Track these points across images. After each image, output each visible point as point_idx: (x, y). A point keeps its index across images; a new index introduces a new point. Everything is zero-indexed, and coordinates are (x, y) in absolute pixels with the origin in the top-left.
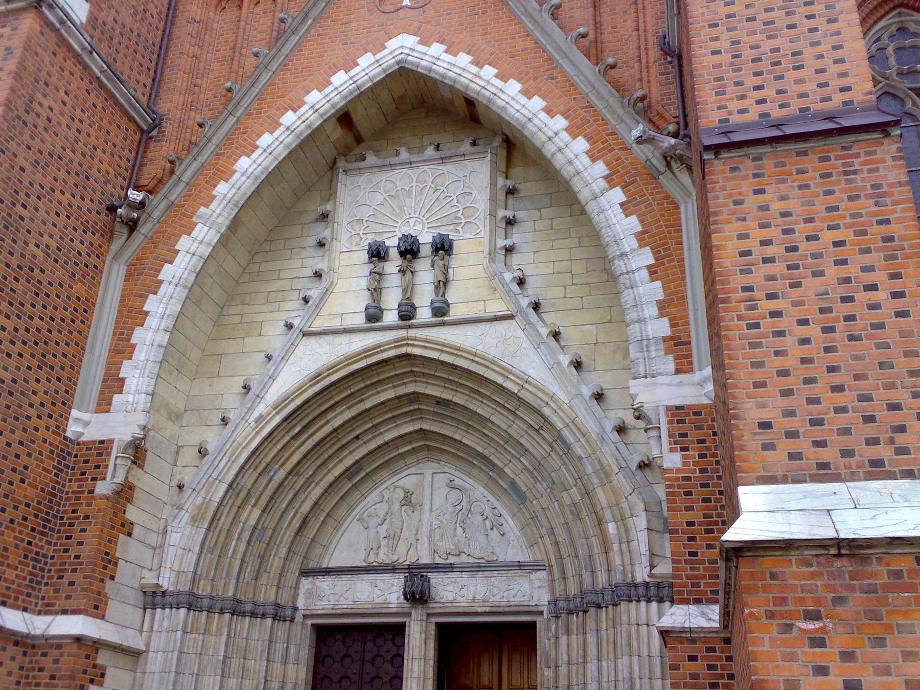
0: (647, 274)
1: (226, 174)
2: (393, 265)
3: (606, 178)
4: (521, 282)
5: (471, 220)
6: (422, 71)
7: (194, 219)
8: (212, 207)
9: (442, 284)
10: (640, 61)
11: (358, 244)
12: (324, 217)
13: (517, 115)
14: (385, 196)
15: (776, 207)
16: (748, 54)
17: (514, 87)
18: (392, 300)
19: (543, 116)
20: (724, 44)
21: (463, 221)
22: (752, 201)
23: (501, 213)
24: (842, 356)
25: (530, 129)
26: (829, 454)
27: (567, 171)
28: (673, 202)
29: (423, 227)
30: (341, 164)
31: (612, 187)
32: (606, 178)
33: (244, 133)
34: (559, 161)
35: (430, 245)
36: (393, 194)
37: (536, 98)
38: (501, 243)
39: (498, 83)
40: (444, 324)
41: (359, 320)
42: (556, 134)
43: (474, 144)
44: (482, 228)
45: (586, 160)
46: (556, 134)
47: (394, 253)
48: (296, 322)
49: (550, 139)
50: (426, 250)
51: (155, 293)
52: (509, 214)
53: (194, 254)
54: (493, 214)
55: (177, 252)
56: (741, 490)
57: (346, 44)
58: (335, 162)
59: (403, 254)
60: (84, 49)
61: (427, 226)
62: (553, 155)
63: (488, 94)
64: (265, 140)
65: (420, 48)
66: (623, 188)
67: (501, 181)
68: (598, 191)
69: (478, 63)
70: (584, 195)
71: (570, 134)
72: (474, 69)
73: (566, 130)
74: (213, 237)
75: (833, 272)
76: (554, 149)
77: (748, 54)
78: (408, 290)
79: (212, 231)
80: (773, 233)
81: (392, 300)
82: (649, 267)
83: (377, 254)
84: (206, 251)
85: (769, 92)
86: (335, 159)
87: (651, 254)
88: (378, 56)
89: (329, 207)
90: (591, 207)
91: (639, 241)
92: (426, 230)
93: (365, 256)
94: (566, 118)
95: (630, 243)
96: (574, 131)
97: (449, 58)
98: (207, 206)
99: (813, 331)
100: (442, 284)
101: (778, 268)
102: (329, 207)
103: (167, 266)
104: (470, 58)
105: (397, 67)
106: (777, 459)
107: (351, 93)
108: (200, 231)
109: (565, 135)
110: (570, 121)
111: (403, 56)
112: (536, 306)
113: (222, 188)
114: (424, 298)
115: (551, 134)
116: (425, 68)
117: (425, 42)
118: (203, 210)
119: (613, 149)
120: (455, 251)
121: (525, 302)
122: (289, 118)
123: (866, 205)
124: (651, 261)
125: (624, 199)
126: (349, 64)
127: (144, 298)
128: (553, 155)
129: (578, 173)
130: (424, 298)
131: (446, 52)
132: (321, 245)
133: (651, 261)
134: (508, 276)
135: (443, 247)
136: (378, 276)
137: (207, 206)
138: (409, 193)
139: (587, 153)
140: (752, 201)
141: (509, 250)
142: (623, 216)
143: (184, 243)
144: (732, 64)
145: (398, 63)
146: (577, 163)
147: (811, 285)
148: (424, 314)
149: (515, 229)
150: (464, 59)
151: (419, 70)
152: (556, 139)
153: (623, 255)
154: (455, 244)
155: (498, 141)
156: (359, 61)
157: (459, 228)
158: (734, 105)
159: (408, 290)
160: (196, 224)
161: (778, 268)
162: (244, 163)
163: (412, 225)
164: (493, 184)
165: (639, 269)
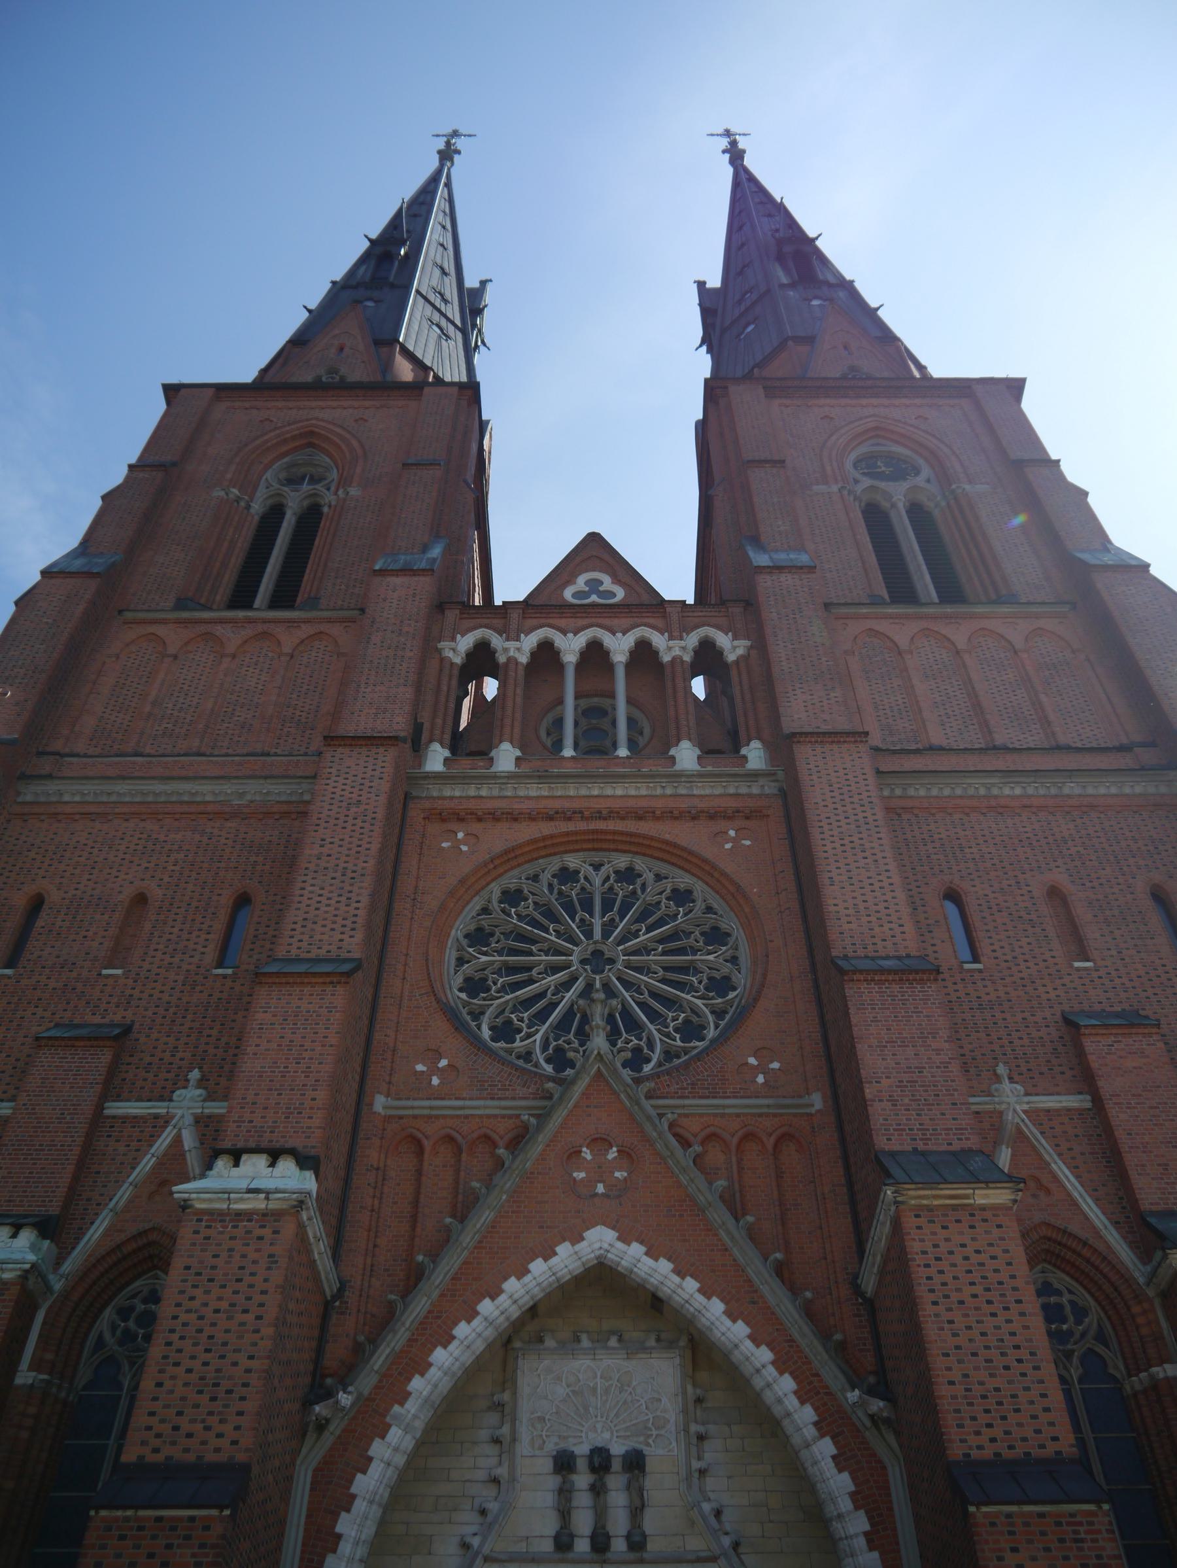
0: (865, 1542)
1: (423, 1367)
2: (582, 1480)
3: (816, 1424)
4: (718, 1513)
5: (662, 1432)
6: (623, 1271)
7: (388, 1419)
8: (408, 1405)
9: (637, 1511)
10: (831, 1294)
11: (541, 1448)
12: (499, 1406)
13: (723, 1338)
14: (567, 1390)
17: (717, 1307)
18: (583, 1523)
19: (749, 1344)
20: (956, 1375)
21: (654, 1433)
23: (694, 1428)
25: (736, 1356)
27: (777, 1411)
28: (880, 1461)
29: (612, 1433)
30: (517, 1344)
31: (822, 1436)
32: (816, 1424)
33: (438, 1317)
34: (768, 1397)
35: (621, 1459)
36: (577, 1389)
37: (740, 1323)
38: (696, 1465)
39: (701, 1298)
40: (641, 1561)
41: (548, 1546)
42: (764, 1366)
43: (658, 1340)
44: (674, 1444)
45: (795, 1402)
46: (764, 1366)
47: (582, 1464)
48: (476, 1542)
49: (758, 1371)
50: (616, 1465)
51: (348, 1510)
52: (701, 1429)
53: (389, 1464)
54: (686, 1430)
55: (370, 1459)
57: (542, 1227)
58: (509, 1341)
59: (593, 1469)
60: (315, 1237)
61: (615, 1434)
62: (762, 1390)
63: (692, 1309)
64: (462, 1330)
65: (619, 1245)
66: (833, 1438)
67: (690, 1388)
68: (809, 1438)
69: (680, 1272)
70: (796, 1440)
71: (777, 1369)
72: (677, 1279)
73: (773, 1363)
74: (408, 1443)
76: (762, 1384)
78: (600, 1513)
79: (408, 1437)
81: (583, 1523)
82: (866, 1534)
83: (564, 1463)
84: (400, 1460)
85: (998, 1432)
86: (510, 1337)
87: (866, 1519)
88: (578, 1247)
89: (506, 1396)
90: (804, 1454)
91: (854, 1501)
92: (615, 1439)
93: (547, 1465)
94: (772, 1350)
95: (846, 1504)
96: (781, 1365)
97: (649, 1261)
98: (402, 1404)
100: (637, 1511)
102: (506, 1396)
103: (359, 1476)
104: (670, 1266)
105: (596, 1262)
107: (550, 1285)
108: (395, 1434)
109: (771, 1371)
110: (775, 1354)
111: (602, 1252)
112: (736, 1545)
113: (417, 1384)
114: (619, 1524)
115: (758, 1365)
116: (626, 1269)
117: (625, 1238)
118: (396, 1408)
119: (818, 1393)
120: (647, 1469)
121: (726, 1541)
122: (486, 1307)
124: (867, 1527)
125: (834, 1451)
126: (549, 1253)
127: (335, 1517)
128: (762, 1390)
129: (788, 1414)
130: (619, 1524)
131: (647, 1254)
132: (497, 1441)
133: (867, 1527)
134: (707, 1507)
135: (635, 1463)
136: (565, 1493)
137: (402, 1404)
138: (594, 1390)
139: (795, 1393)
141: (702, 1472)
142: (835, 1471)
143: (377, 1449)
144: (966, 1397)
145: (597, 1258)
146: (787, 1402)
148: (619, 1545)
149: (707, 1445)
150: (664, 1266)
151: (619, 1269)
152: (764, 1371)
153: (840, 1516)
154: (648, 1460)
155: (683, 1342)
156: (558, 1249)
157: (650, 1441)
158: (973, 1440)
159: (600, 1513)
160: (389, 1426)
162: (440, 1356)
163: (599, 1431)
164: (684, 1393)
165: (857, 1535)
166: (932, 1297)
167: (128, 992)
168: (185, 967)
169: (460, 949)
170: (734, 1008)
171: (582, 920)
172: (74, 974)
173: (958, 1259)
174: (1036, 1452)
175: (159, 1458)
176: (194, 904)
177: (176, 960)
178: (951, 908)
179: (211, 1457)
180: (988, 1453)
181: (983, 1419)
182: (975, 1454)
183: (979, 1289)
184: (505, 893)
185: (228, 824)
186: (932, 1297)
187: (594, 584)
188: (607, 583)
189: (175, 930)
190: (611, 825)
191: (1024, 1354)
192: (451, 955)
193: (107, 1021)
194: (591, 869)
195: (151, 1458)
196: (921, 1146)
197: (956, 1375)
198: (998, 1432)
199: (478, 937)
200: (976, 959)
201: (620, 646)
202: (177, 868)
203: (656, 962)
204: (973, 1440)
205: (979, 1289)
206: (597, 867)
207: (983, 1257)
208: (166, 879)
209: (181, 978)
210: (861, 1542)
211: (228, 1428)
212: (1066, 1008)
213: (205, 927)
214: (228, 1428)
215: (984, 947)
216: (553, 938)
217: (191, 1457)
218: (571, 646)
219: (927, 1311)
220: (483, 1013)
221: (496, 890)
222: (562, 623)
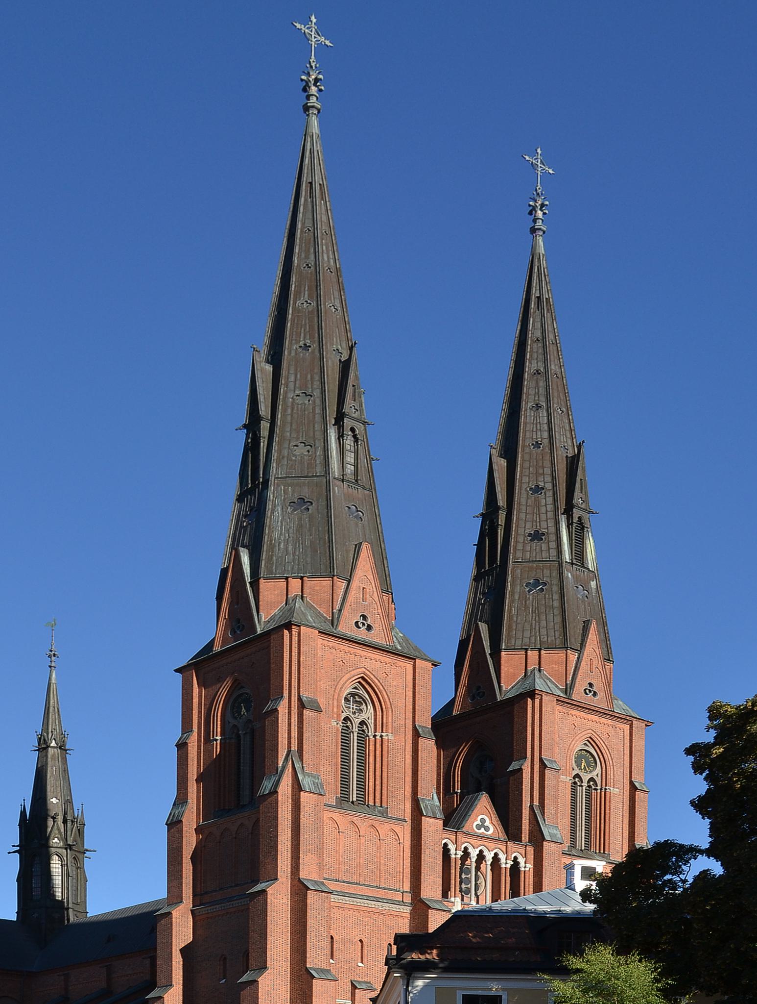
167: (367, 972)
168: (379, 966)
172: (350, 965)
176: (377, 946)
177: (376, 963)
185: (379, 917)
187: (483, 821)
188: (487, 823)
189: (374, 954)
193: (363, 980)
201: (489, 856)
202: (369, 931)
208: (367, 935)
209: (379, 969)
213: (381, 953)
218: (474, 853)
222: (472, 841)
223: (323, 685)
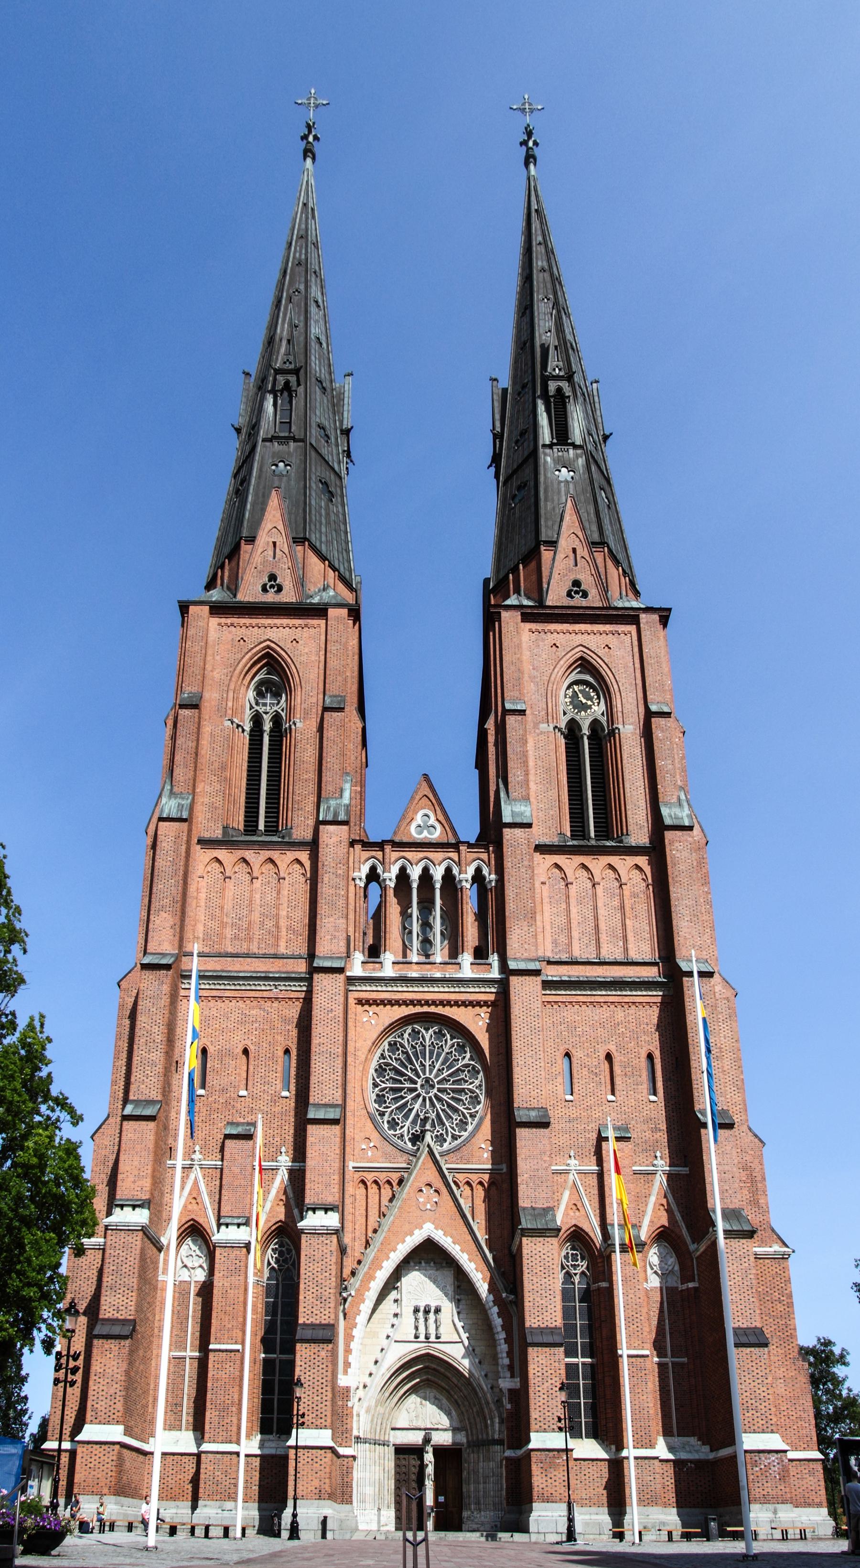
15: (541, 1362)
16: (537, 1304)
20: (531, 1299)
22: (536, 1359)
24: (550, 1404)
26: (546, 1427)
56: (532, 1434)
75: (550, 1381)
77: (537, 1304)
80: (540, 1369)
99: (545, 1396)
101: (540, 1379)
106: (537, 1427)
123: (557, 1364)
140: (536, 1359)
147: (546, 1384)
158: (533, 1321)
161: (540, 1379)
166: (528, 1271)
169: (374, 1079)
170: (476, 1119)
171: (421, 1062)
173: (537, 1257)
174: (550, 1325)
175: (309, 1322)
178: (566, 1060)
179: (323, 1322)
180: (536, 1326)
181: (537, 1314)
182: (533, 1325)
183: (542, 1269)
184: (390, 1044)
186: (528, 1271)
190: (433, 1009)
191: (552, 1292)
192: (371, 1082)
194: (424, 1032)
195: (307, 1322)
196: (534, 1206)
197: (531, 1299)
198: (540, 1318)
199: (381, 1070)
200: (572, 1094)
203: (450, 1089)
204: (533, 1321)
205: (542, 1269)
206: (427, 1030)
207: (545, 1257)
210: (503, 1341)
211: (326, 1312)
212: (601, 1122)
214: (326, 1312)
215: (575, 1090)
216: (409, 1074)
217: (318, 1322)
219: (526, 1276)
220: (384, 1115)
221: (386, 1045)
223: (530, 688)
